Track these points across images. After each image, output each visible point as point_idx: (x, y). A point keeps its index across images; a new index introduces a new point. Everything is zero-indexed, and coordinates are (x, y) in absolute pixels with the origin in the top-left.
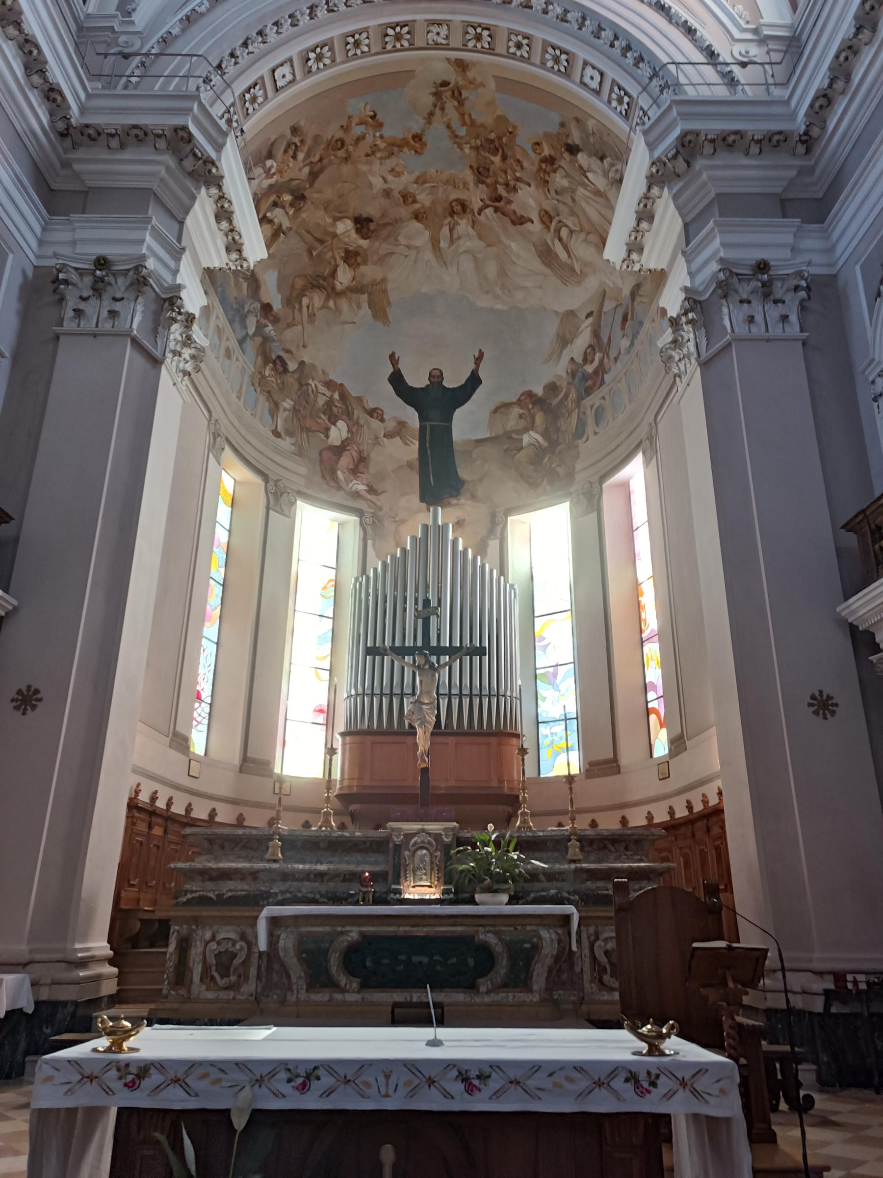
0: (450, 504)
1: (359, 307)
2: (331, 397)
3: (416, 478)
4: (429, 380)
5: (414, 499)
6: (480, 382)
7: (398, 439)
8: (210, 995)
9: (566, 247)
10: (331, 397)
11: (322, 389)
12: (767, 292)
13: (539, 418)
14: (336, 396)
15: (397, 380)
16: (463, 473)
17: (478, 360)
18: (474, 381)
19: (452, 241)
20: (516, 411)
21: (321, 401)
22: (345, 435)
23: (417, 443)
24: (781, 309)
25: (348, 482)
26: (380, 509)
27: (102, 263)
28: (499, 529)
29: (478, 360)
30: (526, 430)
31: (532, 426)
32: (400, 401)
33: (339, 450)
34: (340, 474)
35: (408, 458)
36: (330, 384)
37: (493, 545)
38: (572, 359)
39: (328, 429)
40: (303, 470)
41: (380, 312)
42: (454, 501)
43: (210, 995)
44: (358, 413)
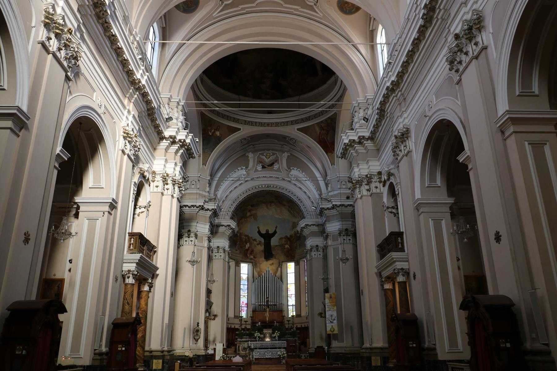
0: (270, 260)
1: (251, 218)
2: (246, 238)
3: (263, 254)
4: (266, 231)
5: (263, 259)
6: (276, 232)
7: (259, 245)
8: (243, 353)
9: (293, 212)
10: (246, 238)
11: (244, 237)
12: (317, 250)
13: (289, 242)
14: (247, 238)
15: (259, 232)
16: (274, 253)
17: (276, 228)
18: (275, 232)
19: (270, 206)
20: (284, 240)
21: (244, 240)
22: (249, 246)
23: (263, 246)
24: (320, 252)
25: (250, 256)
26: (256, 261)
27: (218, 247)
28: (281, 266)
29: (276, 228)
30: (286, 244)
31: (287, 244)
32: (260, 237)
33: (247, 250)
34: (248, 255)
35: (262, 249)
36: (246, 236)
37: (279, 269)
38: (295, 232)
39: (246, 245)
40: (241, 256)
41: (255, 219)
42: (271, 259)
43: (243, 353)
44: (251, 241)
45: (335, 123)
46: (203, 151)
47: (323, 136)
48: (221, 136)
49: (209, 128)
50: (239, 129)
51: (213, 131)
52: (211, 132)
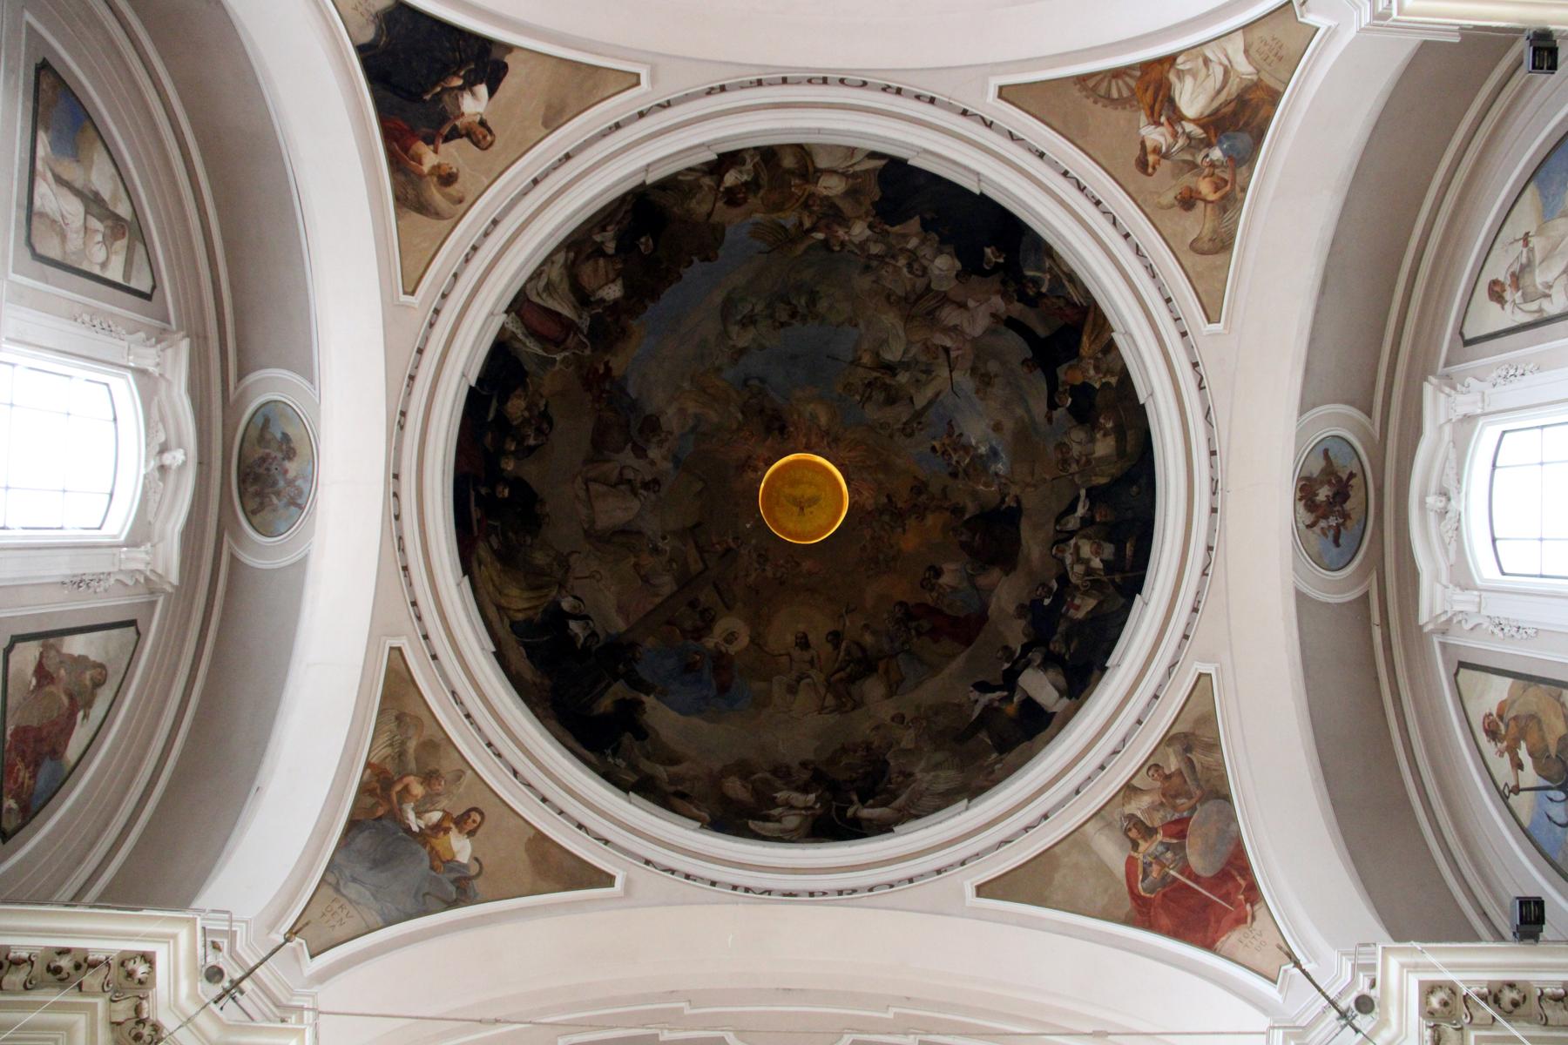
45: (1214, 746)
46: (331, 878)
47: (1155, 872)
48: (479, 874)
49: (418, 790)
50: (606, 880)
51: (436, 816)
52: (419, 815)
